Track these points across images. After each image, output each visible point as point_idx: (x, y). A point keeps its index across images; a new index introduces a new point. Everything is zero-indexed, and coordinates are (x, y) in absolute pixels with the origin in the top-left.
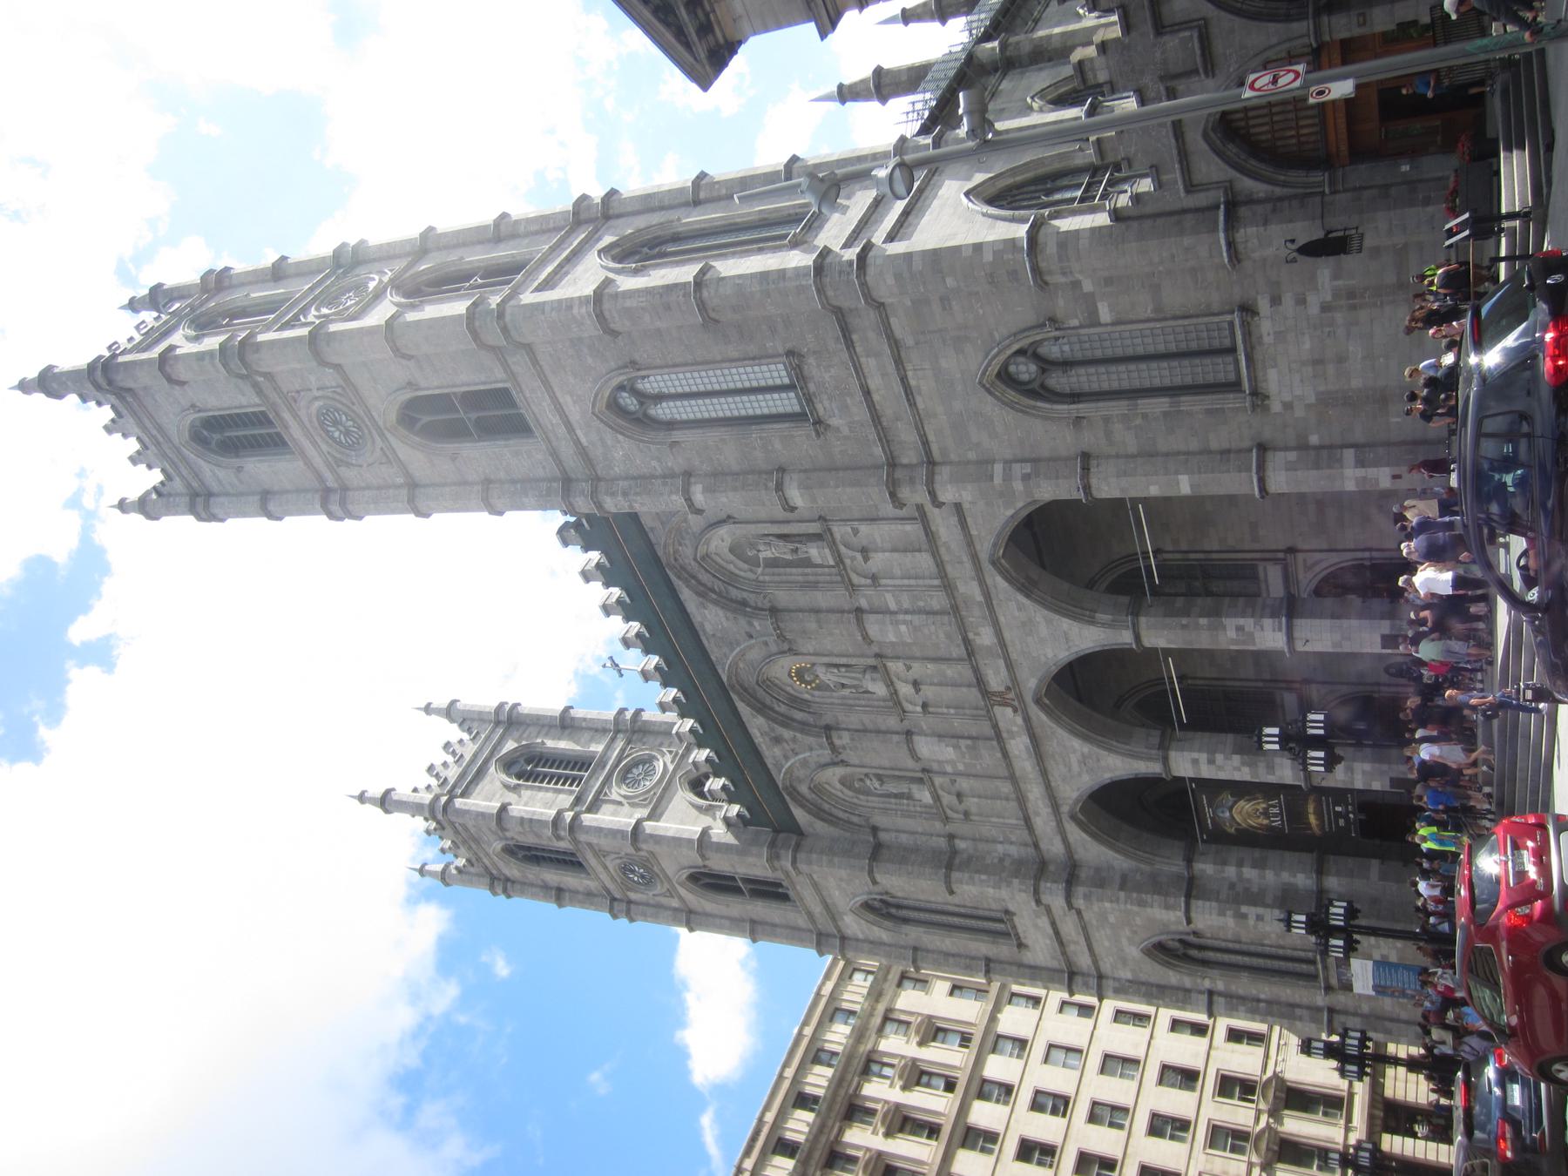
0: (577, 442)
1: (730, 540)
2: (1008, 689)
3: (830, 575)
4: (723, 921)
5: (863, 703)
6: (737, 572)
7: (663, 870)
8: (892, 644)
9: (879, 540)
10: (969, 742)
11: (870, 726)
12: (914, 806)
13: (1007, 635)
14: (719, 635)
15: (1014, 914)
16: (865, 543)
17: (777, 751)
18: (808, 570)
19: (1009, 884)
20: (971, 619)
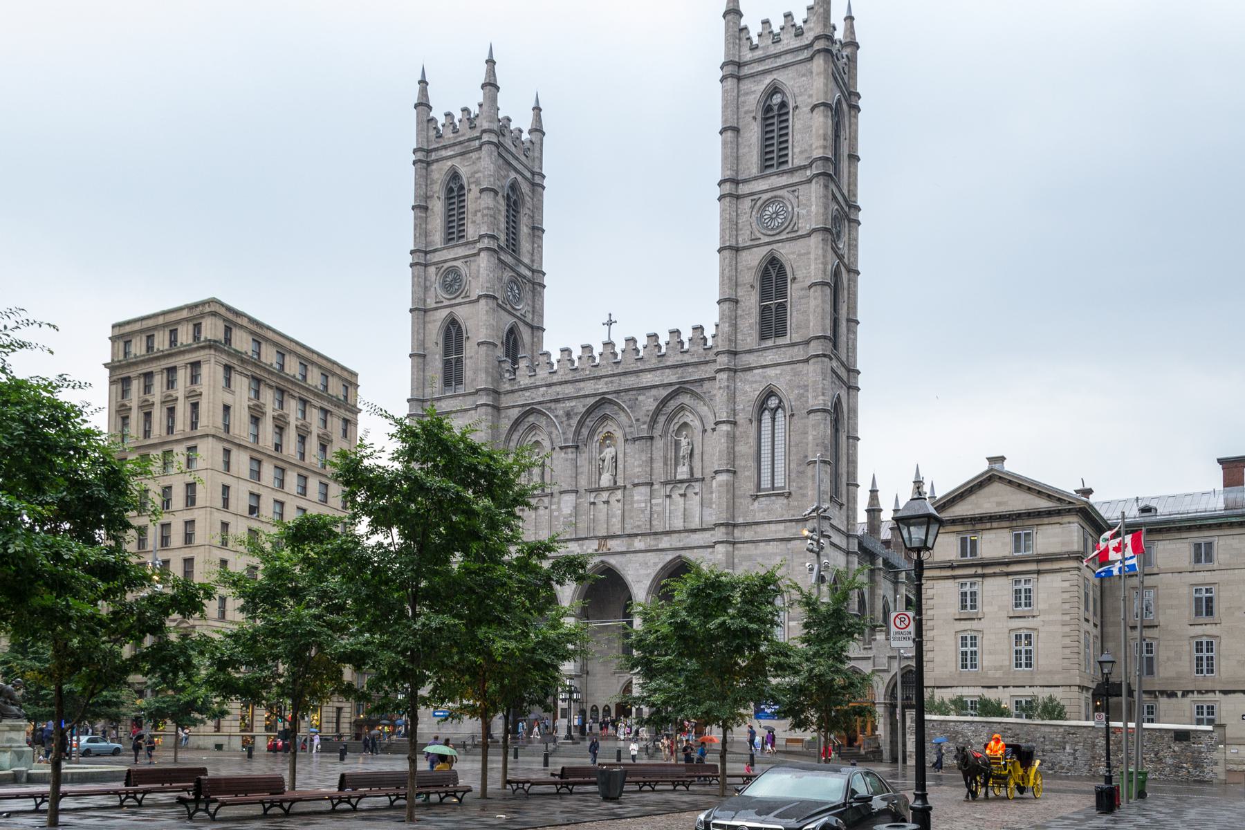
0: (756, 368)
1: (691, 424)
8: (633, 496)
11: (580, 470)
17: (560, 413)
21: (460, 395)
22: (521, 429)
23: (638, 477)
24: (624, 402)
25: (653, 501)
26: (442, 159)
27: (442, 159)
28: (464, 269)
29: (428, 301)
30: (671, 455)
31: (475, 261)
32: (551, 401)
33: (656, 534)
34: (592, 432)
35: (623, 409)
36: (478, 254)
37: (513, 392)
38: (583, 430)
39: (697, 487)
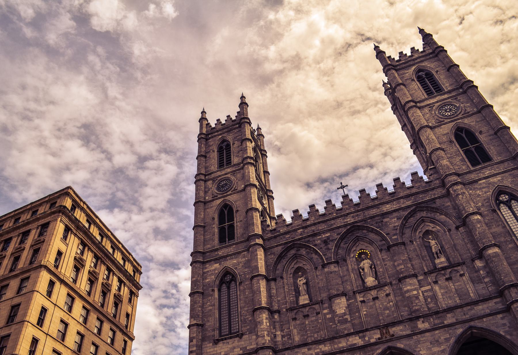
0: (480, 180)
1: (434, 230)
2: (393, 335)
3: (429, 266)
4: (203, 215)
6: (418, 232)
7: (231, 194)
8: (401, 289)
9: (457, 284)
10: (349, 320)
12: (293, 297)
13: (427, 334)
14: (383, 223)
15: (241, 338)
16: (454, 278)
18: (428, 258)
19: (268, 335)
20: (432, 319)
21: (233, 244)
22: (284, 261)
23: (402, 273)
24: (372, 225)
25: (423, 289)
26: (216, 136)
27: (216, 136)
28: (233, 178)
29: (207, 198)
30: (425, 253)
31: (241, 172)
32: (309, 236)
33: (437, 313)
34: (348, 251)
35: (372, 231)
36: (242, 168)
37: (275, 237)
38: (340, 251)
39: (461, 270)
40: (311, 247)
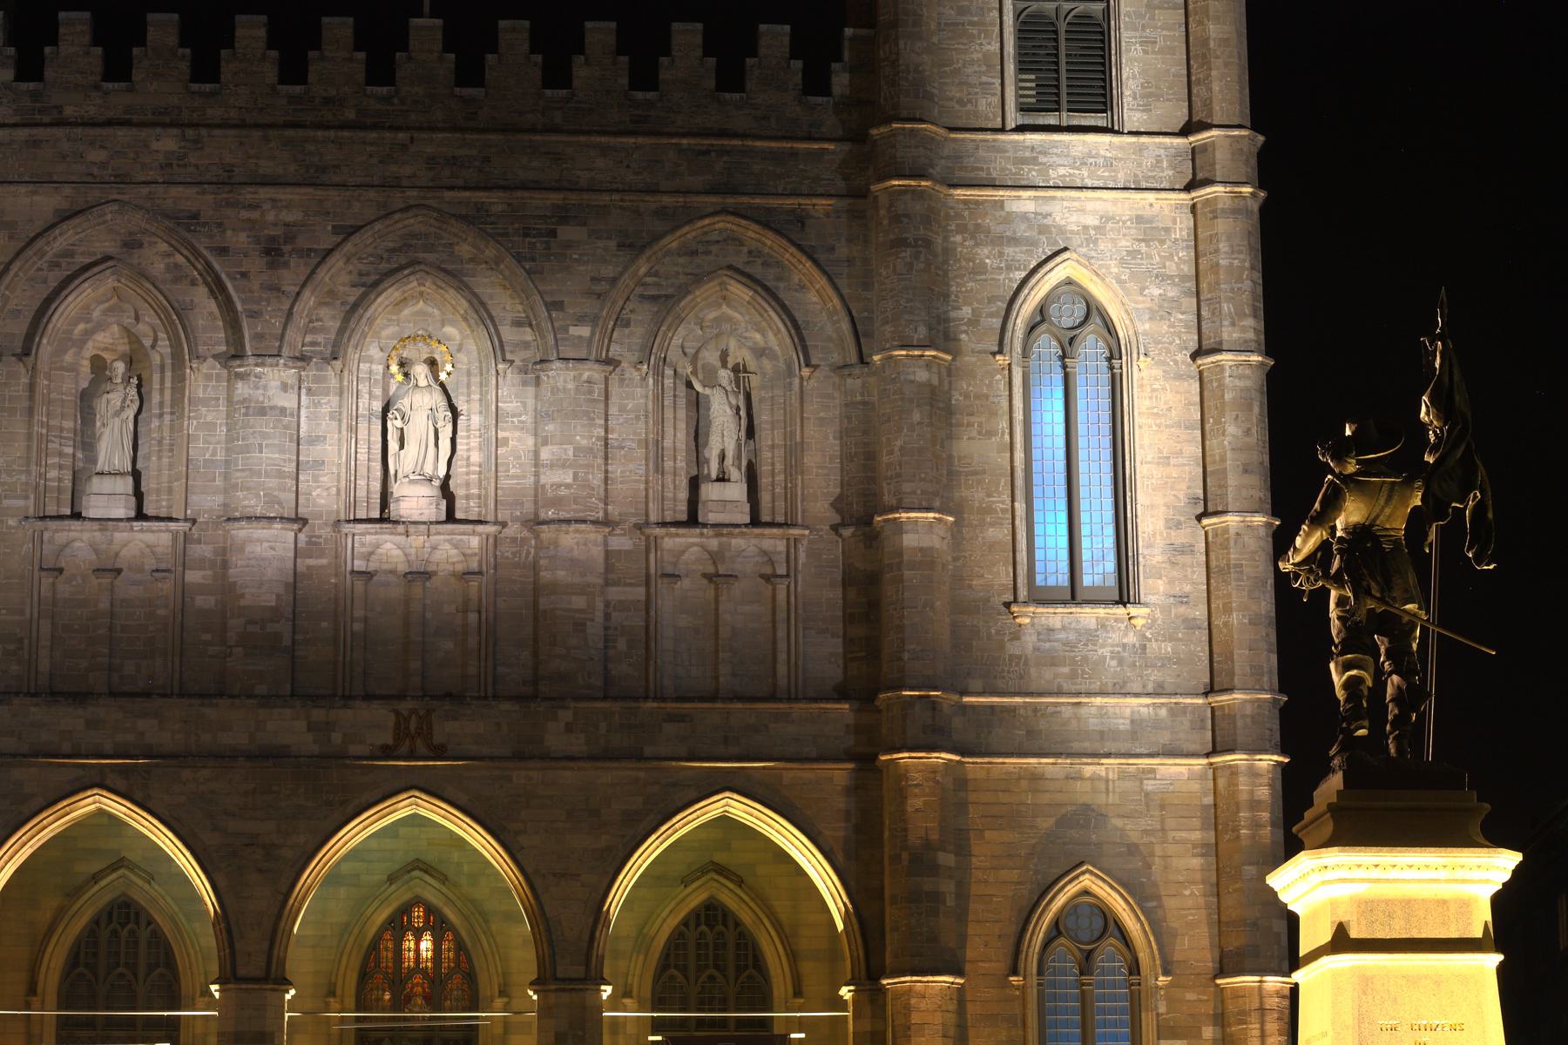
5: (362, 457)
10: (287, 641)
12: (61, 467)
40: (198, 255)
